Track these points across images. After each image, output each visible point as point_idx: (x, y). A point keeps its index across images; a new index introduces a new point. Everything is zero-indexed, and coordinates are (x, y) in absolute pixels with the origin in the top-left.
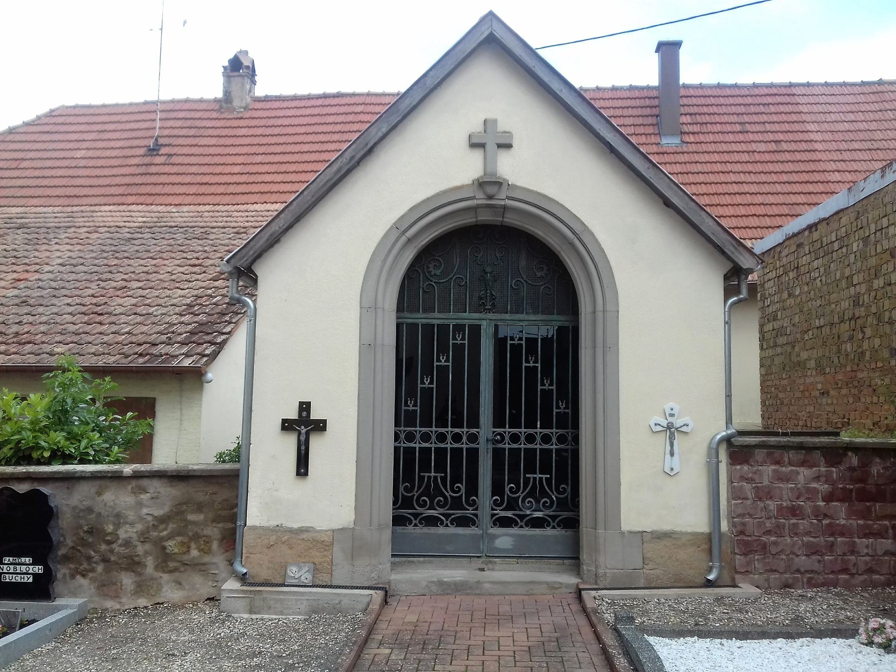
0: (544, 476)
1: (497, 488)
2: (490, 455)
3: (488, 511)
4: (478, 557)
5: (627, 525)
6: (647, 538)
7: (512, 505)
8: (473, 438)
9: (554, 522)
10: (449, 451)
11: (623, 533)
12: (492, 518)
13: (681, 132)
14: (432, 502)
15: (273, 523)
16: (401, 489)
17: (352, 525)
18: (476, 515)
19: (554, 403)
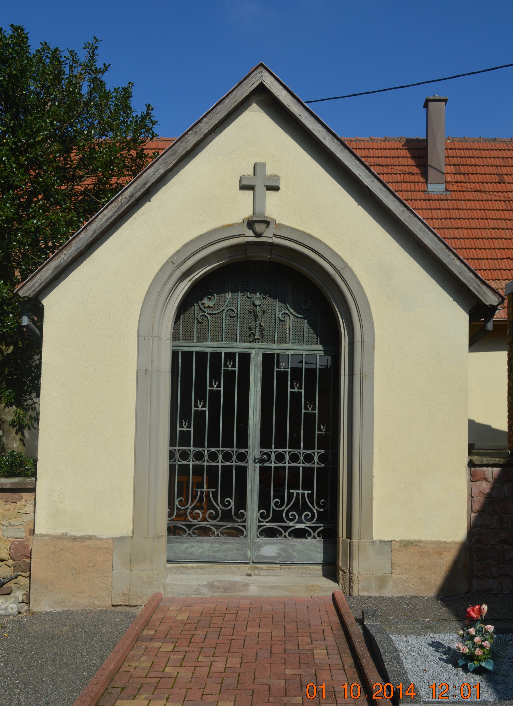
0: (306, 492)
1: (264, 503)
2: (257, 472)
3: (256, 523)
4: (246, 563)
5: (376, 536)
6: (395, 546)
7: (277, 517)
8: (242, 457)
9: (314, 532)
10: (220, 468)
11: (374, 542)
12: (258, 529)
13: (446, 182)
14: (300, 516)
15: (59, 532)
16: (177, 502)
17: (130, 534)
18: (244, 527)
19: (317, 426)
